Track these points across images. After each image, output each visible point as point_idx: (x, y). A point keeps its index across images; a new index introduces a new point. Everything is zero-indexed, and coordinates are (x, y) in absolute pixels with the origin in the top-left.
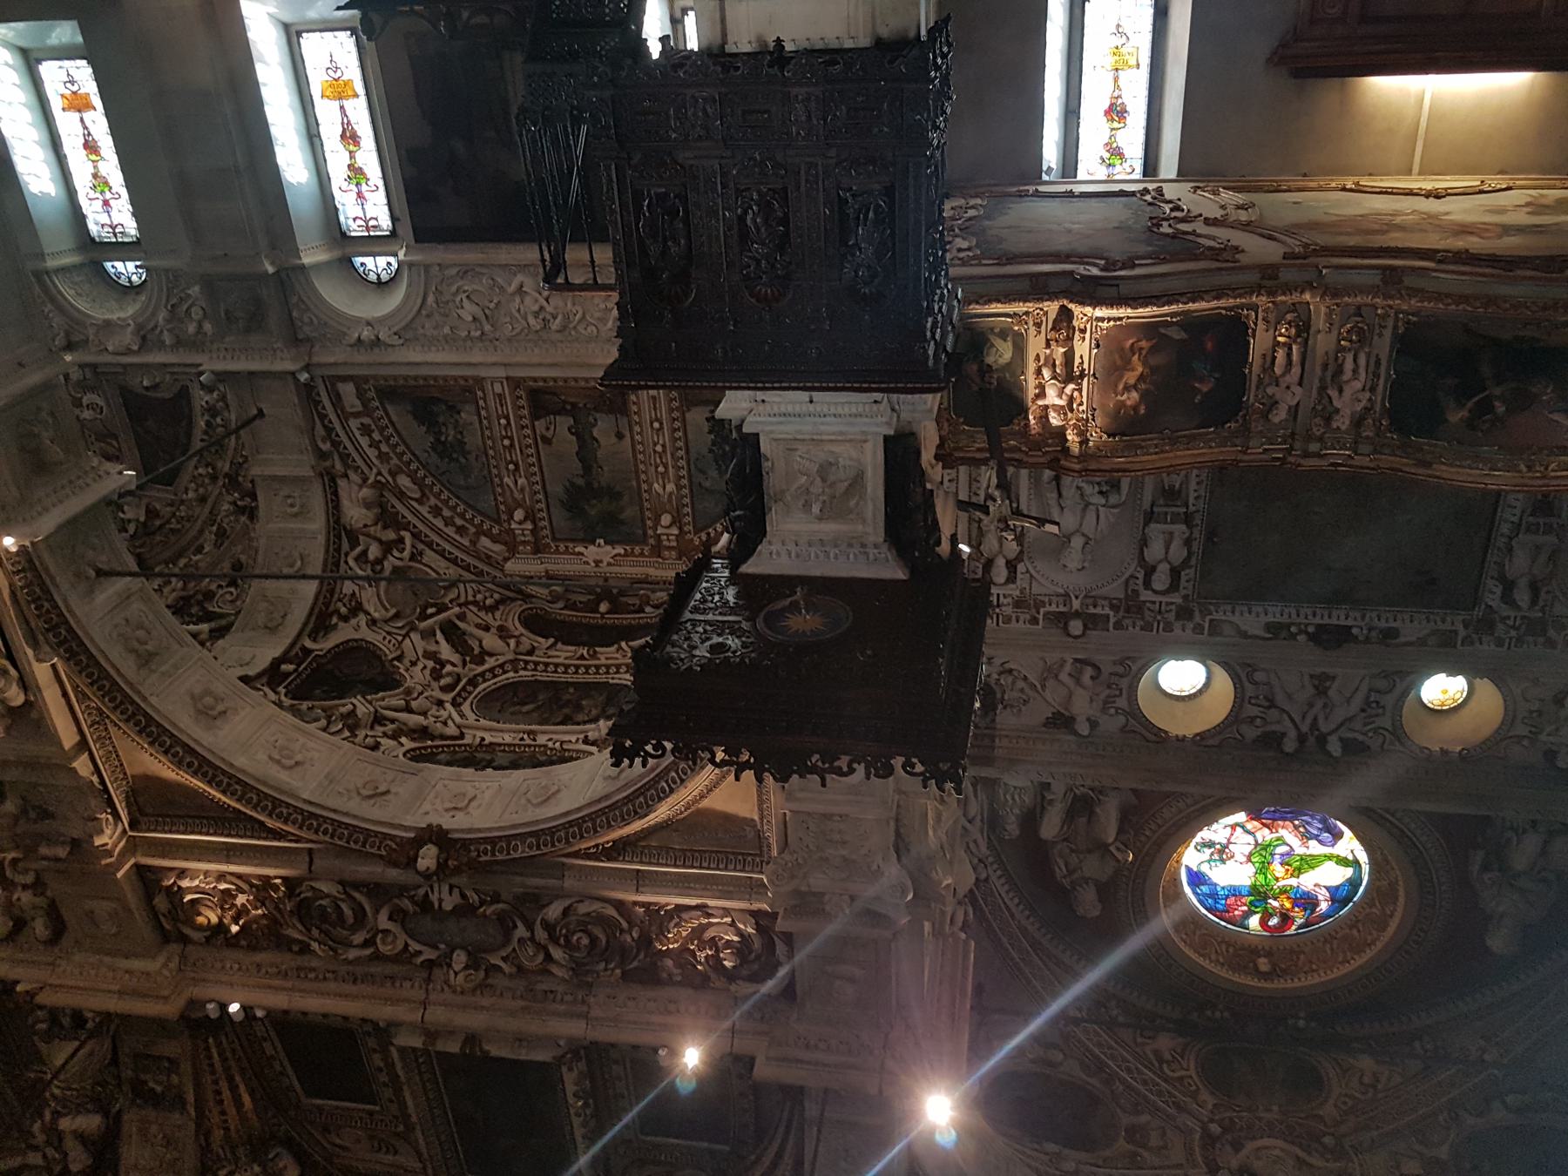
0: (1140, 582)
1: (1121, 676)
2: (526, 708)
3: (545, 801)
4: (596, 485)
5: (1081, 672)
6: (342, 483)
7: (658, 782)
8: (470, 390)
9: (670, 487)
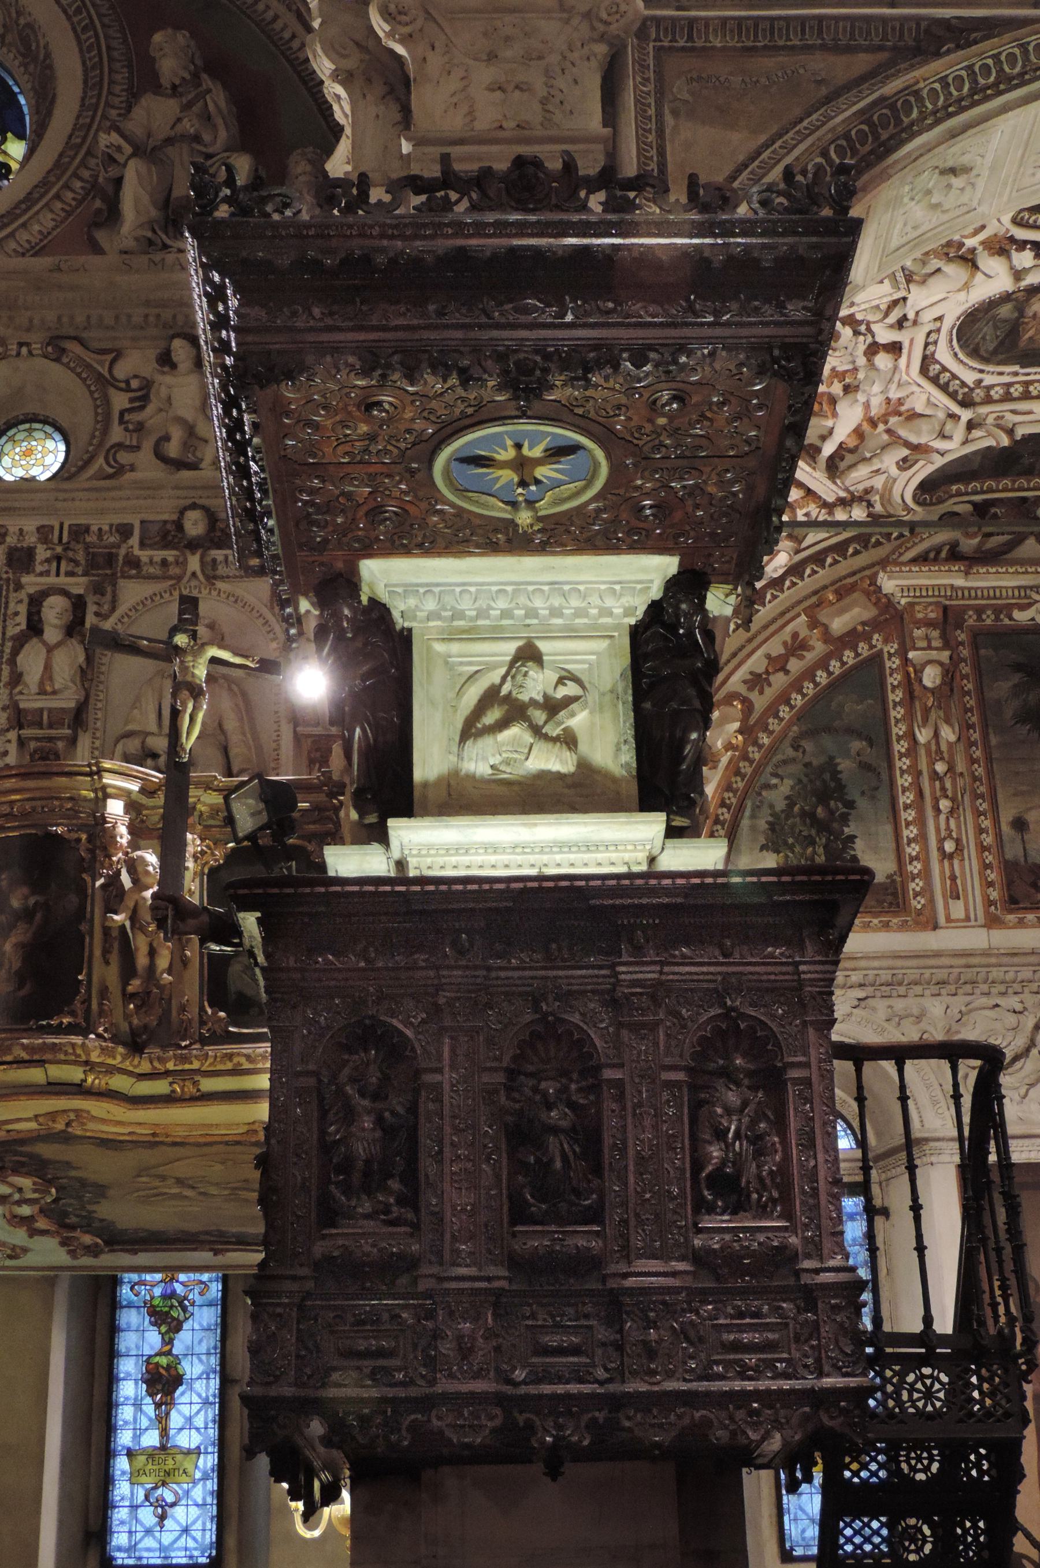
0: (91, 608)
1: (119, 446)
5: (186, 446)
9: (923, 736)
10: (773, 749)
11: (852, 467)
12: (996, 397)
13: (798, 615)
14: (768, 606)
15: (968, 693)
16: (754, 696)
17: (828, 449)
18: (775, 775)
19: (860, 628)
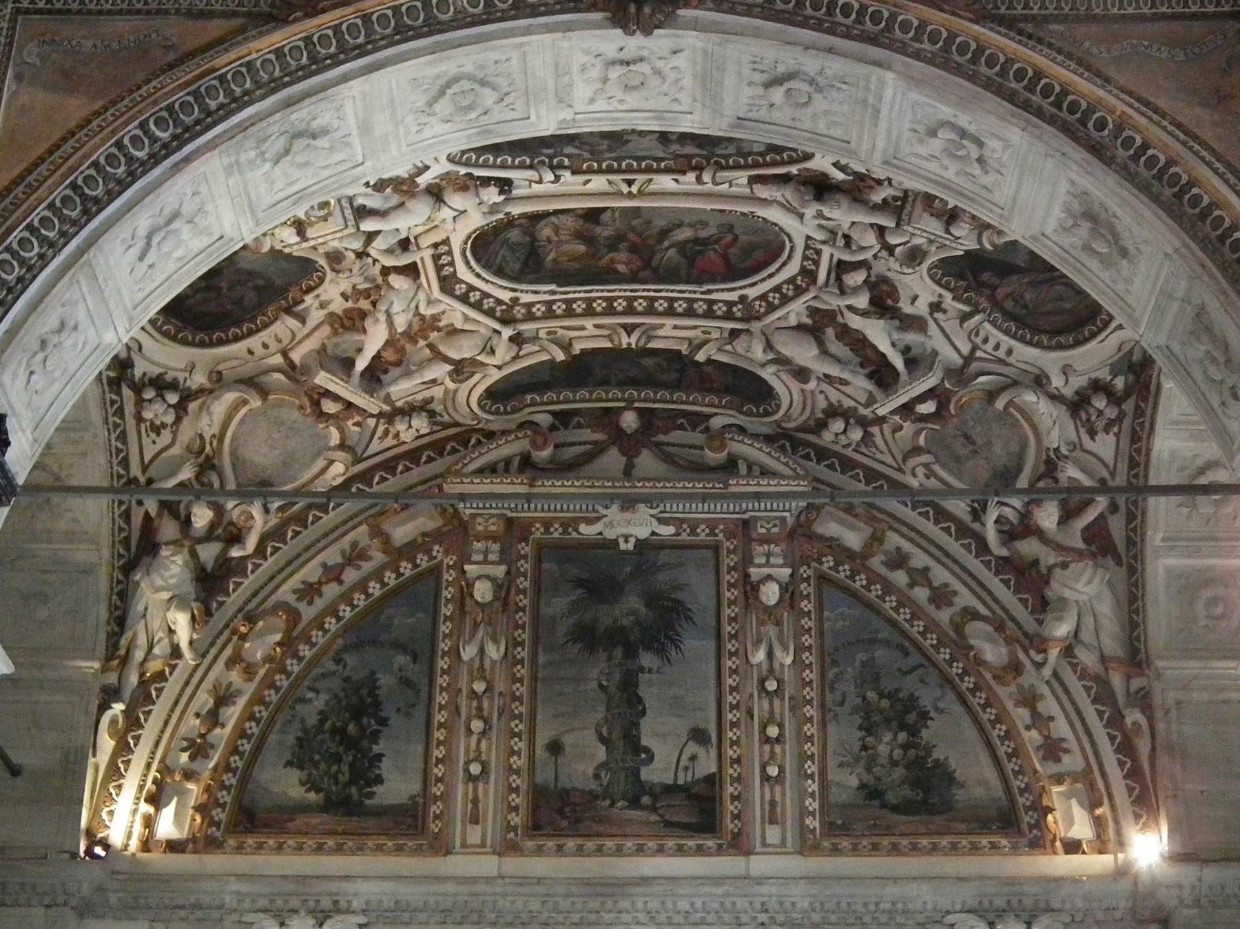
2: (684, 234)
3: (449, 85)
4: (618, 652)
6: (1112, 646)
7: (175, 137)
8: (831, 828)
9: (469, 652)
11: (394, 381)
12: (539, 314)
13: (360, 524)
14: (332, 514)
15: (523, 609)
16: (302, 607)
17: (361, 364)
19: (420, 540)
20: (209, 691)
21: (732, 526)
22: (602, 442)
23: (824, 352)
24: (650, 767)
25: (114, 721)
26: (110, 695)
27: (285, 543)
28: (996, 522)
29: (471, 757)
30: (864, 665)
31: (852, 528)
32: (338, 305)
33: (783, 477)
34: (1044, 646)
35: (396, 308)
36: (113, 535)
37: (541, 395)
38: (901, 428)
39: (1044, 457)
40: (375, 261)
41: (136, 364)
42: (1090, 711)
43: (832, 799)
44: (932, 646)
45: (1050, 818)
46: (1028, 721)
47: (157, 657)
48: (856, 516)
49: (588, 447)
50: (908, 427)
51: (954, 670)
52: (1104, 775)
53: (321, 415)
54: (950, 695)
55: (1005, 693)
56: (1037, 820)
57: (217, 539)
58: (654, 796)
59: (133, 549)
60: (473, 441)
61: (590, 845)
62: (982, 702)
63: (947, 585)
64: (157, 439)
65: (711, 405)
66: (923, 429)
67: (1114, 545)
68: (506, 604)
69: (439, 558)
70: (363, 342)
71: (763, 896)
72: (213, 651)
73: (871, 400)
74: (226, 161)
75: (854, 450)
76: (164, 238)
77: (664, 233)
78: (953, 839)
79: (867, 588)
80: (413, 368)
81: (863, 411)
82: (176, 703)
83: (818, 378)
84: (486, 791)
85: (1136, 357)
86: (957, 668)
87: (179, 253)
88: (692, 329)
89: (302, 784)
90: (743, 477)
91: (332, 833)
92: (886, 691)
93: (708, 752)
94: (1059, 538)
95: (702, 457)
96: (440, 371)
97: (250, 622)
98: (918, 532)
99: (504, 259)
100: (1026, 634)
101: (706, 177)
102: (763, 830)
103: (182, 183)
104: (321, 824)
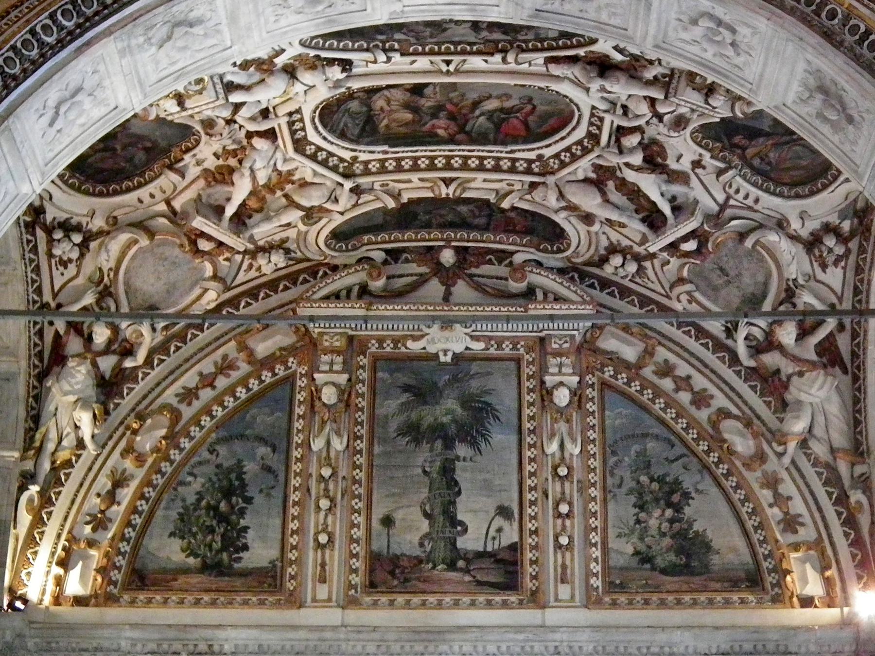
2: (491, 105)
4: (439, 444)
6: (840, 440)
7: (79, 26)
8: (611, 587)
9: (318, 444)
10: (193, 452)
11: (257, 225)
12: (374, 170)
13: (230, 340)
14: (206, 332)
16: (183, 407)
17: (230, 210)
18: (191, 474)
20: (107, 476)
21: (531, 343)
22: (426, 274)
23: (607, 201)
24: (465, 537)
25: (31, 500)
26: (28, 478)
27: (169, 355)
28: (746, 339)
29: (320, 528)
30: (638, 454)
31: (629, 344)
32: (211, 163)
33: (572, 302)
34: (783, 440)
35: (258, 165)
36: (30, 350)
37: (376, 236)
38: (668, 262)
39: (785, 286)
40: (241, 127)
41: (47, 210)
42: (821, 492)
43: (612, 563)
44: (693, 439)
45: (788, 578)
46: (772, 500)
47: (65, 448)
48: (632, 334)
49: (415, 278)
50: (674, 262)
51: (711, 459)
52: (832, 544)
53: (197, 252)
54: (708, 480)
55: (753, 478)
56: (778, 581)
57: (114, 352)
58: (468, 561)
59: (46, 361)
60: (321, 273)
61: (416, 600)
62: (734, 484)
63: (705, 390)
64: (65, 272)
65: (515, 244)
66: (685, 264)
67: (842, 360)
68: (348, 405)
69: (293, 369)
70: (231, 193)
71: (555, 641)
72: (111, 444)
73: (644, 240)
74: (120, 45)
75: (630, 280)
76: (69, 108)
77: (476, 104)
78: (710, 595)
79: (641, 392)
80: (272, 214)
81: (637, 249)
82: (81, 485)
83: (601, 222)
84: (332, 557)
85: (860, 204)
86: (713, 458)
87: (82, 120)
88: (498, 182)
89: (183, 551)
90: (540, 303)
91: (207, 591)
92: (656, 476)
93: (511, 525)
94: (797, 351)
95: (507, 286)
96: (294, 216)
97: (140, 420)
98: (682, 347)
99: (346, 125)
100: (770, 430)
101: (510, 58)
102: (556, 587)
103: (84, 63)
104: (198, 583)
